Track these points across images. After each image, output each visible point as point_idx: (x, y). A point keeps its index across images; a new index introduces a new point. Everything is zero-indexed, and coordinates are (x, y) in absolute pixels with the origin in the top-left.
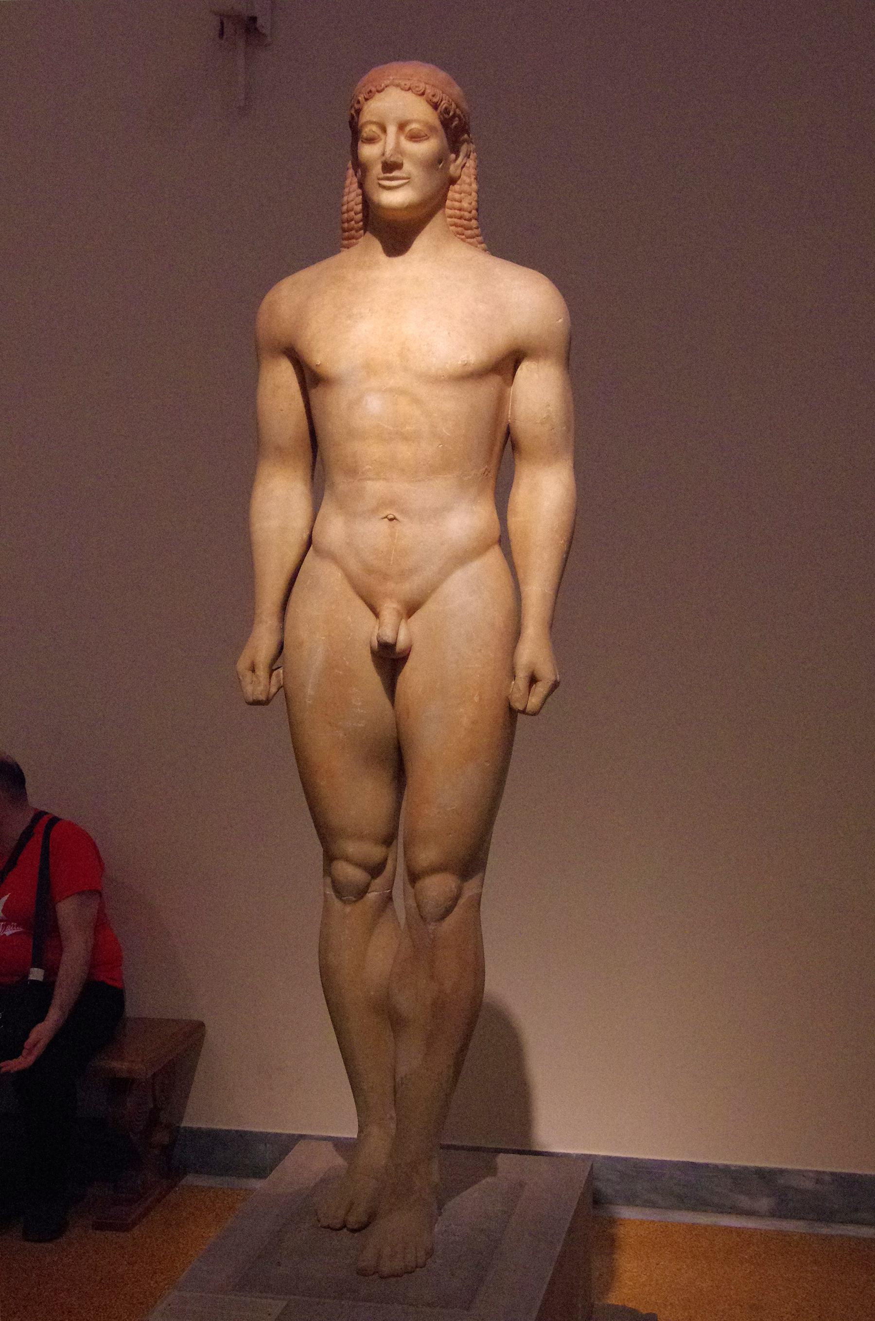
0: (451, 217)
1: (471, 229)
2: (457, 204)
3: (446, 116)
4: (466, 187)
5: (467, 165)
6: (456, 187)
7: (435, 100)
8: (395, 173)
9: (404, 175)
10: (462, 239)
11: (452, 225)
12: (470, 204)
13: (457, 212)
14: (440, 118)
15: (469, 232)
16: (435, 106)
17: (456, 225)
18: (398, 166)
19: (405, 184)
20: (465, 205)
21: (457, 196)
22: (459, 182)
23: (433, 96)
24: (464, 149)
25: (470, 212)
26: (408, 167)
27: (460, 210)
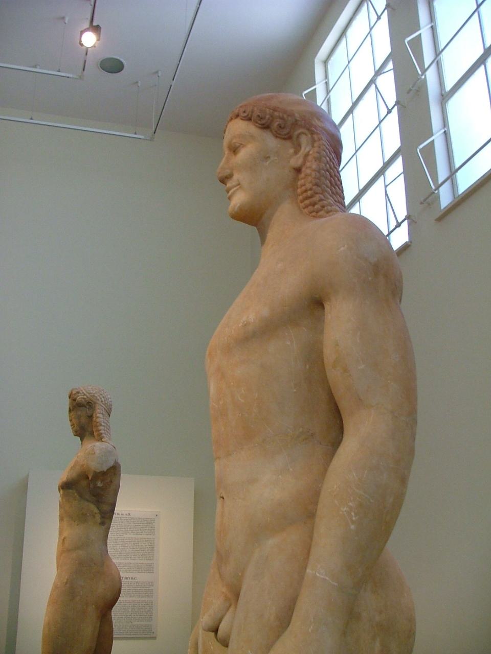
0: (302, 202)
1: (314, 204)
2: (303, 188)
3: (263, 122)
4: (308, 171)
5: (311, 153)
6: (302, 175)
7: (245, 115)
8: (229, 185)
9: (234, 184)
10: (314, 217)
11: (304, 208)
12: (311, 182)
13: (305, 195)
14: (257, 126)
15: (316, 207)
16: (249, 119)
17: (306, 207)
18: (230, 177)
19: (237, 189)
20: (308, 186)
21: (303, 181)
22: (303, 169)
23: (244, 112)
24: (304, 140)
25: (311, 189)
26: (236, 176)
27: (306, 191)
